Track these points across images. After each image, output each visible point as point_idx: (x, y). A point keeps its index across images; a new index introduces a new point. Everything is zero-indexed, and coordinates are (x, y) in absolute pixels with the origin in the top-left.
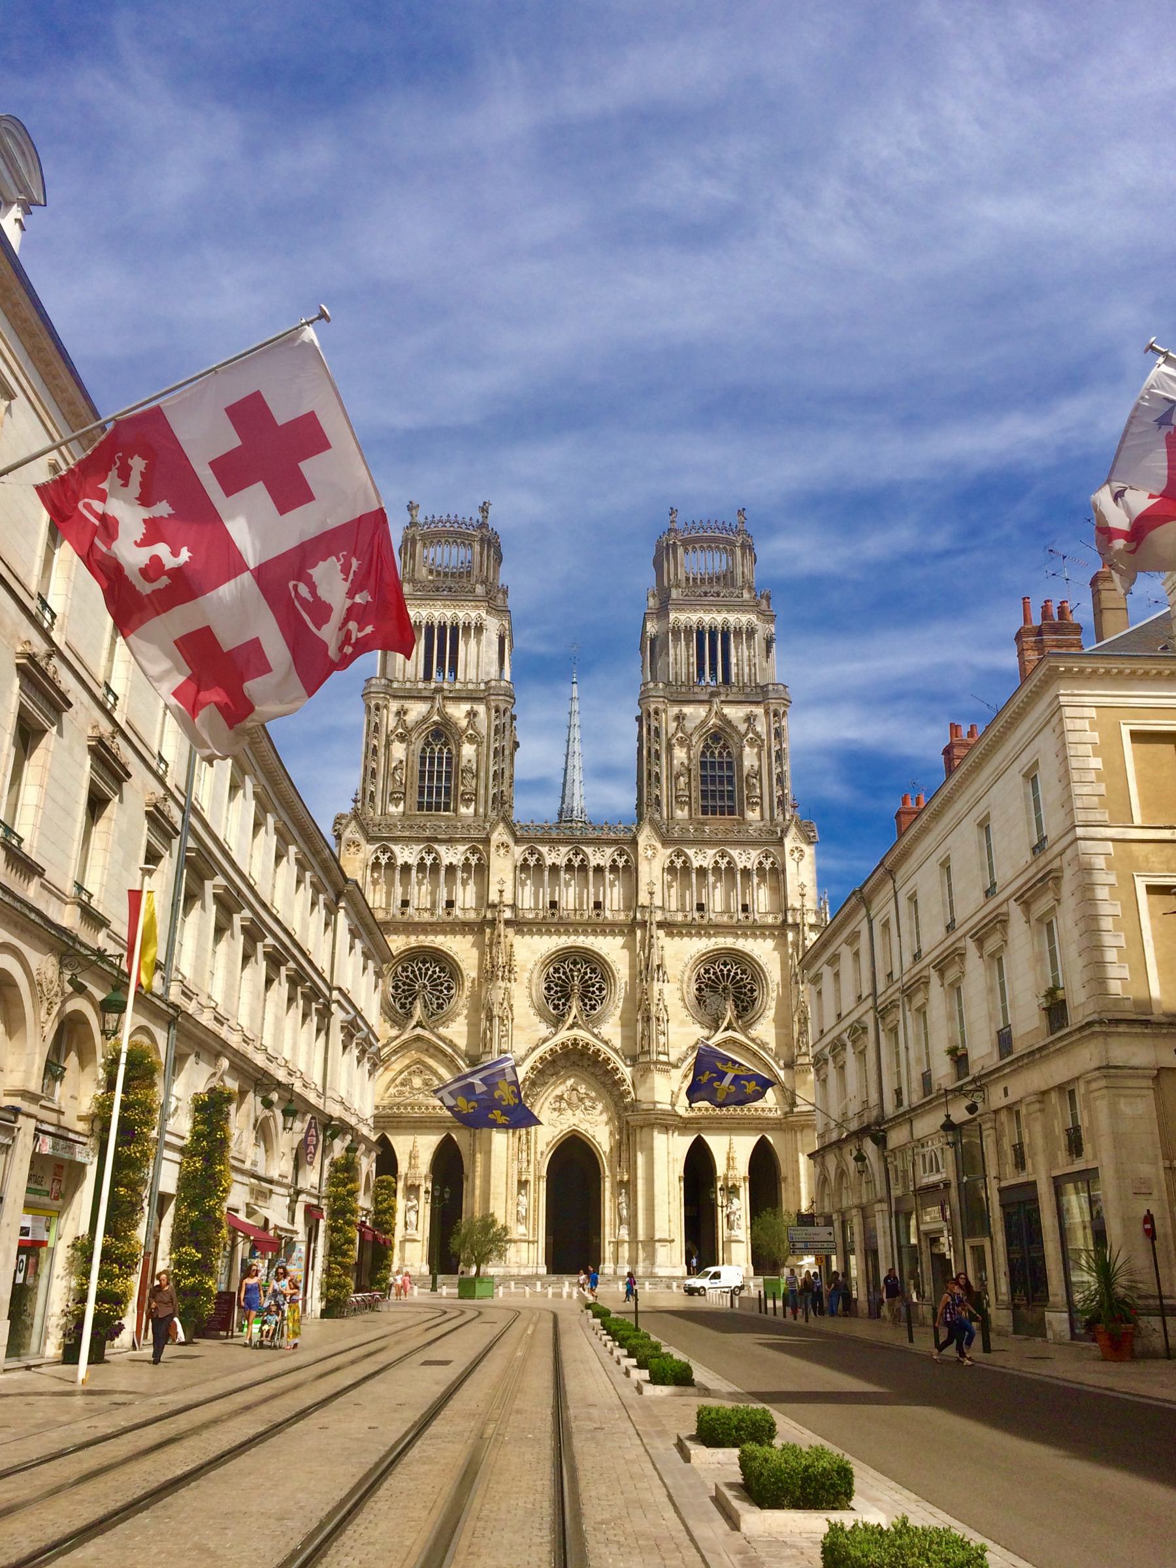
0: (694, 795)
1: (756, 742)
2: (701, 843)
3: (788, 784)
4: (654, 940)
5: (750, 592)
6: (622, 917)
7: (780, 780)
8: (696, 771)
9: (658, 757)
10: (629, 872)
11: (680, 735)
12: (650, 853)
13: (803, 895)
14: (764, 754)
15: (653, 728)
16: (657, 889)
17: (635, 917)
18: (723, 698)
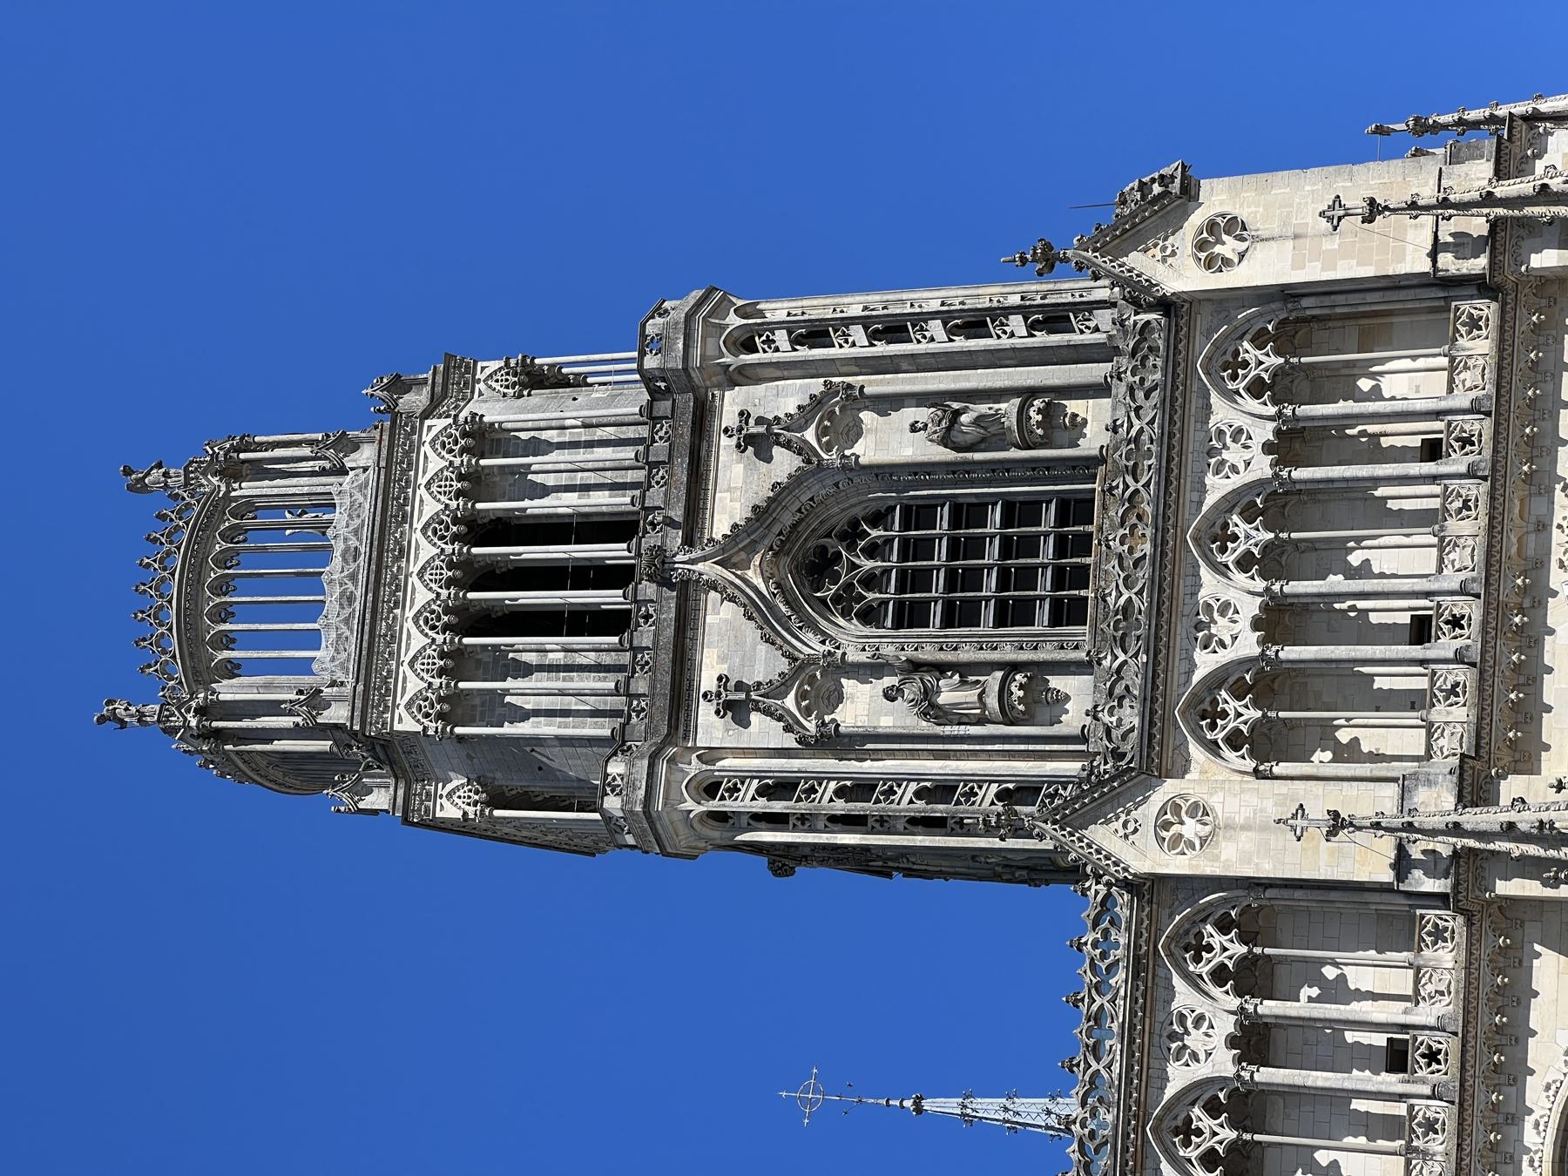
0: (1008, 654)
1: (838, 412)
2: (1168, 619)
3: (984, 296)
4: (1525, 820)
5: (356, 446)
6: (1445, 958)
7: (975, 324)
8: (927, 642)
9: (861, 789)
10: (1271, 922)
11: (790, 702)
12: (1190, 829)
13: (1374, 210)
14: (877, 385)
15: (762, 805)
16: (1320, 801)
17: (1440, 899)
18: (676, 538)
